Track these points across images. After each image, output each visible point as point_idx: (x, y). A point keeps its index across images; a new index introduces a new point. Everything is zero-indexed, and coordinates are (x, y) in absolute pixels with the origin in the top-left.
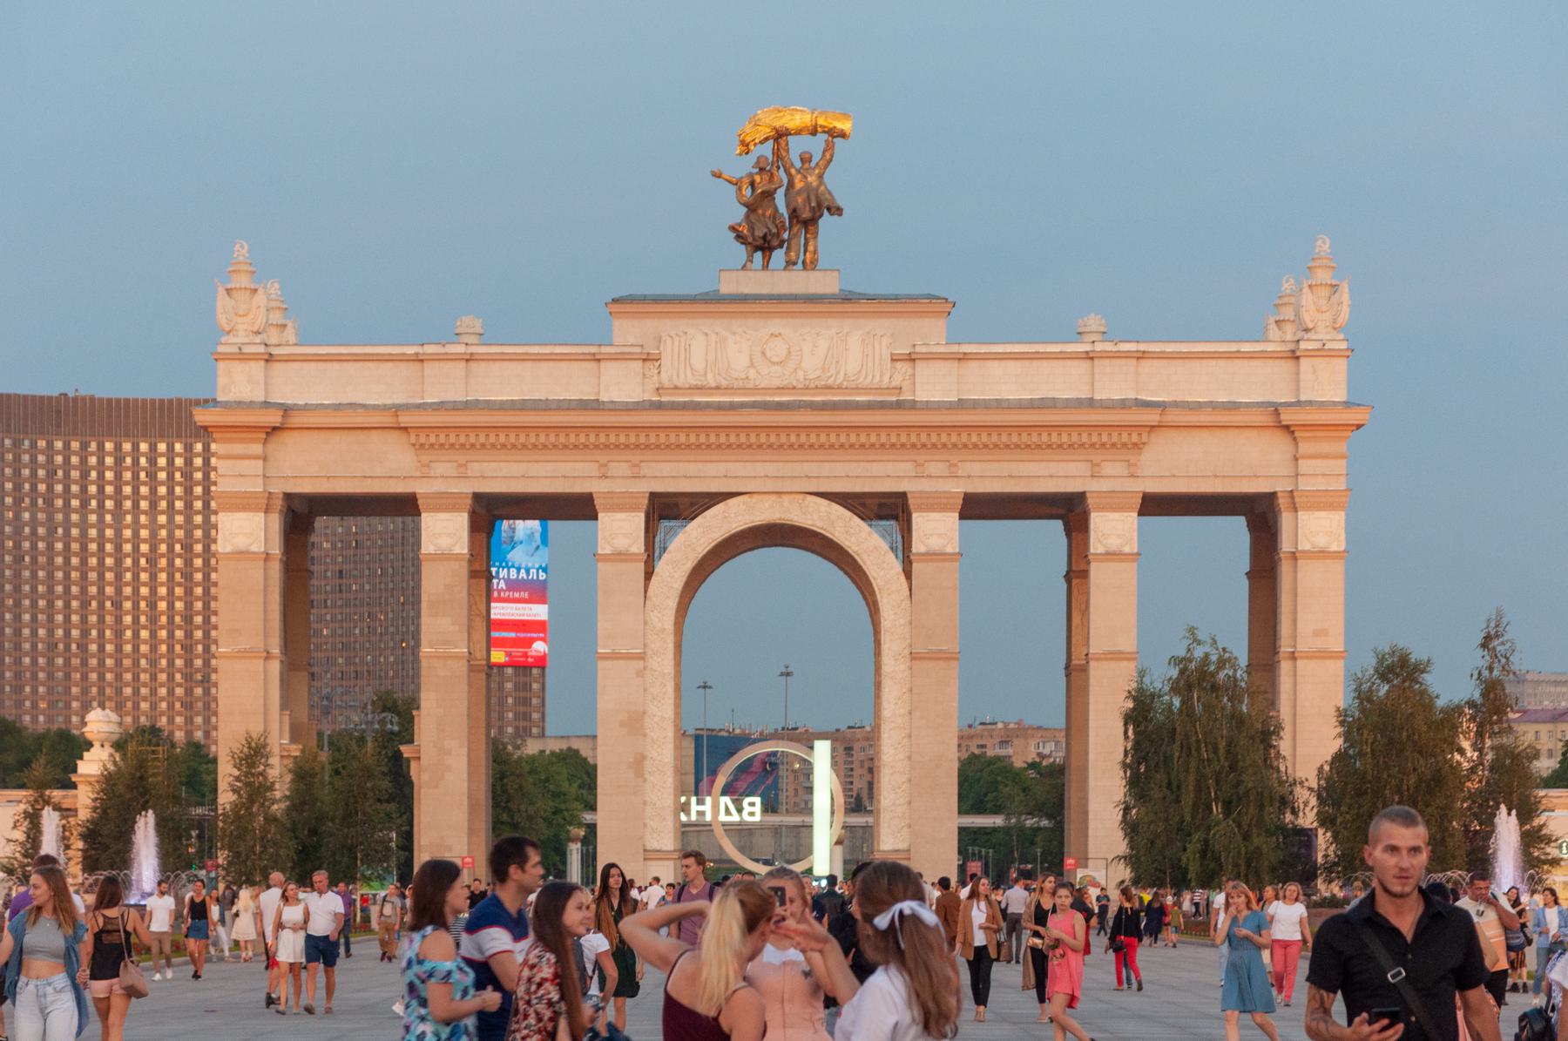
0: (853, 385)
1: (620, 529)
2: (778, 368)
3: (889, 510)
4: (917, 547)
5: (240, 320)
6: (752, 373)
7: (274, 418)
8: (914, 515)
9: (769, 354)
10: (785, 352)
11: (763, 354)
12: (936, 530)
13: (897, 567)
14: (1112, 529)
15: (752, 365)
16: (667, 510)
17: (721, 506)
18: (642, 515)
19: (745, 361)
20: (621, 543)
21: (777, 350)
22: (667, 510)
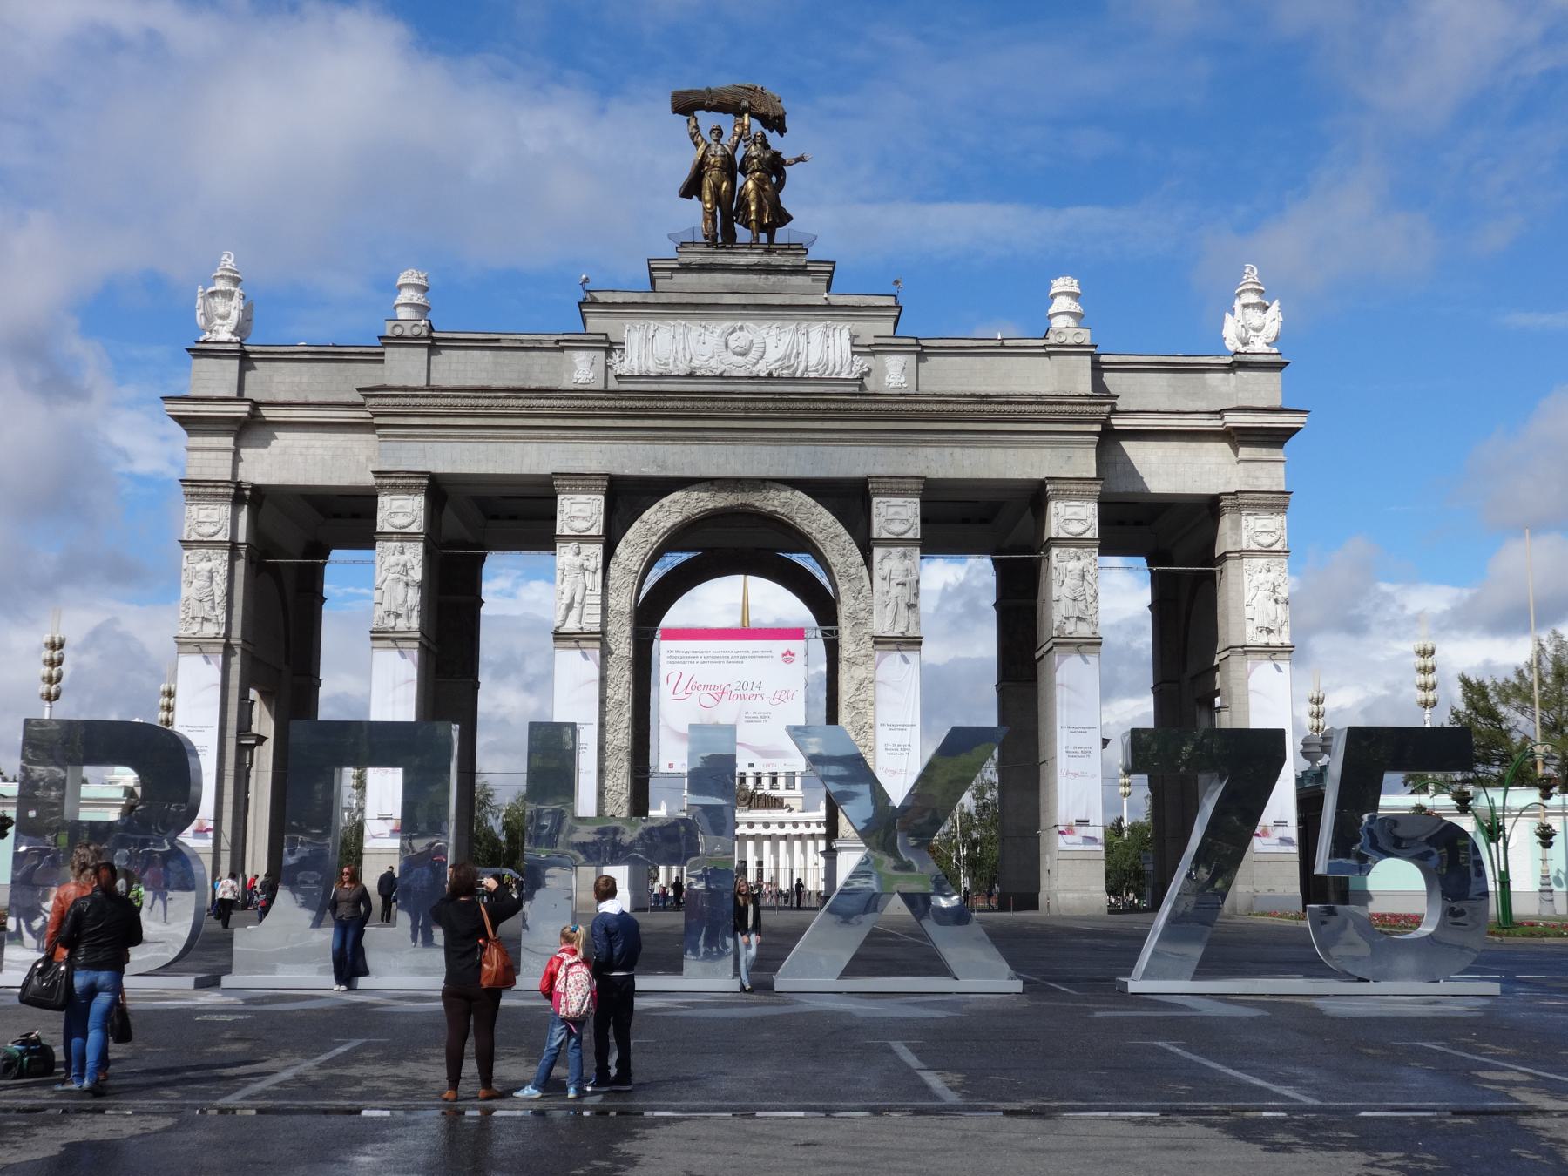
0: (812, 375)
1: (580, 512)
2: (740, 358)
3: (850, 500)
4: (878, 531)
5: (218, 321)
6: (713, 363)
7: (242, 410)
8: (875, 500)
9: (732, 344)
11: (727, 346)
12: (896, 515)
14: (1072, 517)
18: (602, 497)
20: (580, 525)
21: (739, 340)
22: (626, 498)
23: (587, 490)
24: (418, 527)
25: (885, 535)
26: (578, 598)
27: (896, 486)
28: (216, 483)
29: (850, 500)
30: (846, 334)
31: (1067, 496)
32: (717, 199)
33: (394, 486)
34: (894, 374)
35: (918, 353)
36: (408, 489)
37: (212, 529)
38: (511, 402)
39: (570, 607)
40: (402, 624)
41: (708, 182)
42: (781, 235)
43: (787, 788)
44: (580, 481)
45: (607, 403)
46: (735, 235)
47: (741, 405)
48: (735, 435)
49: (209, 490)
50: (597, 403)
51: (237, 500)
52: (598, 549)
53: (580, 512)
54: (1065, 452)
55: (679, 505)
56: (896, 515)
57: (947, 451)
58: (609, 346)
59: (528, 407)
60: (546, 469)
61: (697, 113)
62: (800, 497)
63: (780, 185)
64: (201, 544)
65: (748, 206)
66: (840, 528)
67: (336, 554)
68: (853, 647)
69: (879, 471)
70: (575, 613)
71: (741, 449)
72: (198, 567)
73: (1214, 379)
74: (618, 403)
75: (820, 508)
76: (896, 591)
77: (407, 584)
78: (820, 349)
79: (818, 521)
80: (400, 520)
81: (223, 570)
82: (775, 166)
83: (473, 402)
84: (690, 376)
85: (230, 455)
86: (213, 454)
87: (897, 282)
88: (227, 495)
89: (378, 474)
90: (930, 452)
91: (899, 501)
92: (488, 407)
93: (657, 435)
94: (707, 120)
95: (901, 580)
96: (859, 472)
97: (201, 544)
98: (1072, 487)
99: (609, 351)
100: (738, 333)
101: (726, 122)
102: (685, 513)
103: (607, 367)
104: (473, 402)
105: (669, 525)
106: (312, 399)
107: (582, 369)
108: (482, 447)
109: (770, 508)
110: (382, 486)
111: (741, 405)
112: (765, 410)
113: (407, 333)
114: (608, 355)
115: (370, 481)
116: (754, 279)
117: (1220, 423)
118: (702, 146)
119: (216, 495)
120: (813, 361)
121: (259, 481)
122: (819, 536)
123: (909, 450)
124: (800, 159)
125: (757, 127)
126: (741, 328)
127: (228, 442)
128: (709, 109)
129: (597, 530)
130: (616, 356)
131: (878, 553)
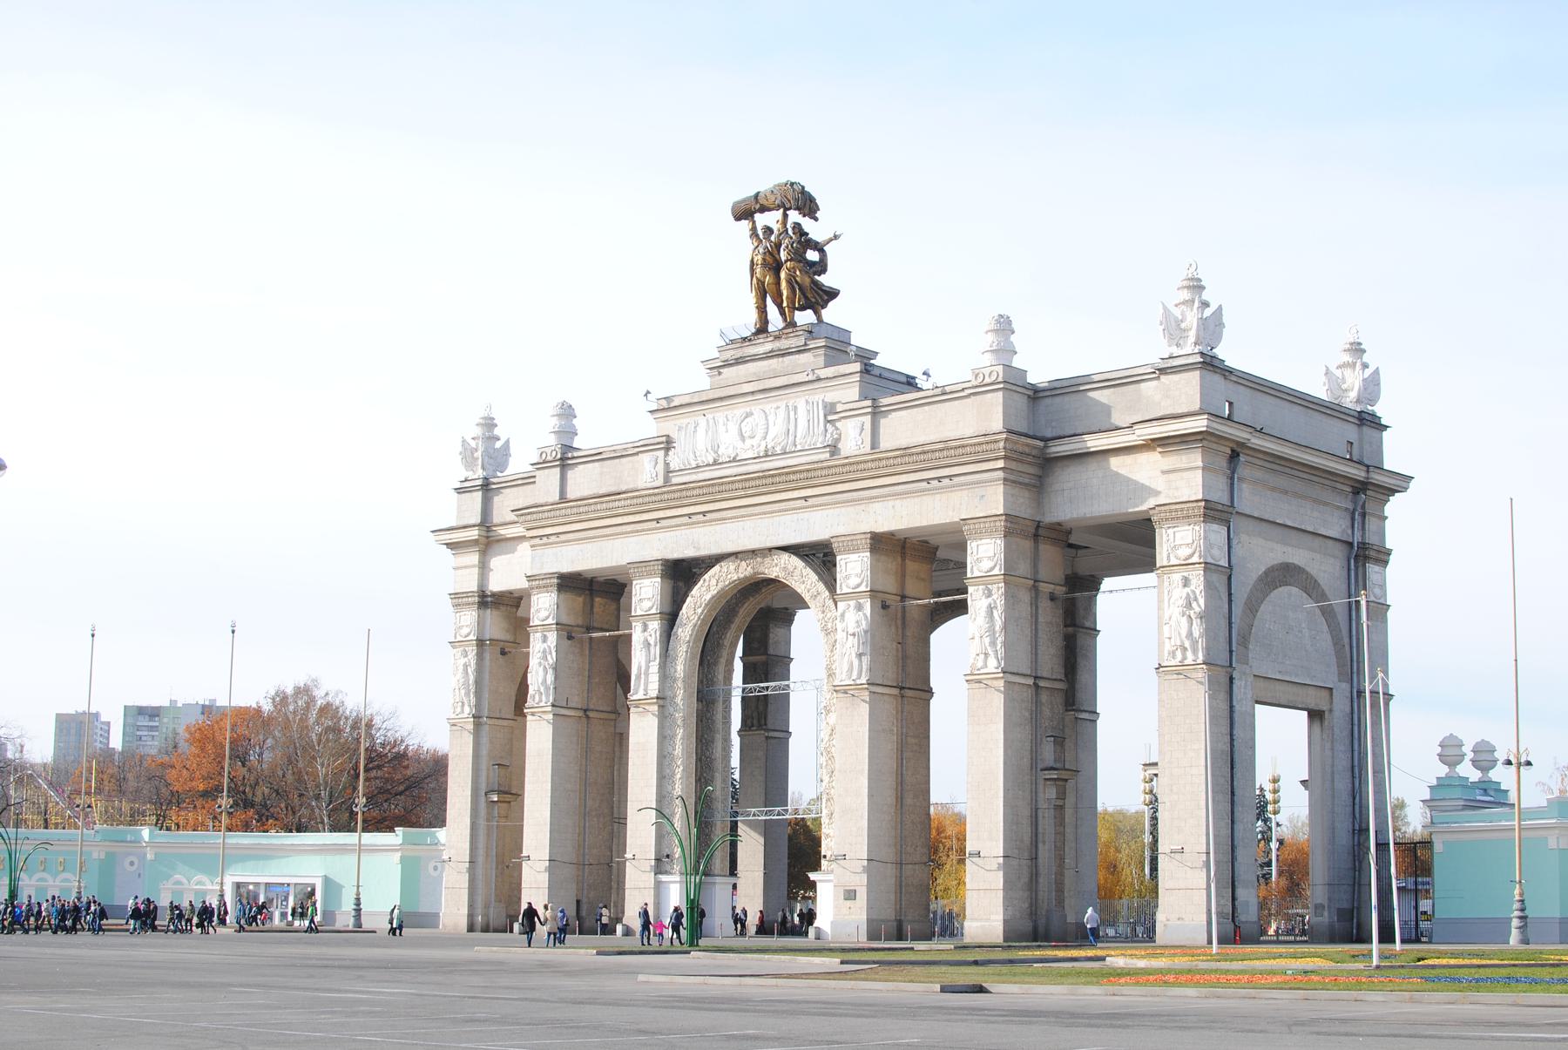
12: (854, 569)
17: (717, 568)
31: (980, 534)
34: (853, 437)
39: (639, 677)
44: (643, 566)
53: (647, 594)
54: (979, 491)
55: (714, 582)
56: (854, 569)
57: (891, 503)
61: (757, 216)
62: (795, 562)
63: (821, 267)
66: (821, 587)
67: (1108, 583)
69: (841, 530)
71: (748, 524)
73: (1148, 388)
75: (809, 570)
81: (473, 663)
85: (476, 570)
89: (530, 578)
94: (762, 220)
98: (980, 524)
99: (667, 449)
102: (721, 585)
103: (667, 464)
105: (708, 597)
114: (666, 455)
115: (524, 584)
116: (774, 363)
117: (1134, 437)
124: (836, 237)
125: (794, 216)
128: (763, 209)
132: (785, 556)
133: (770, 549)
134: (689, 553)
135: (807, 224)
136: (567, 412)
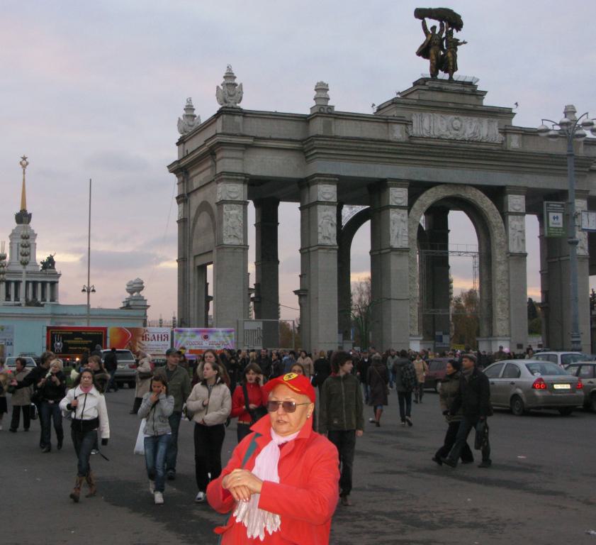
0: (485, 141)
1: (398, 195)
2: (457, 132)
3: (497, 194)
6: (448, 133)
7: (250, 141)
9: (455, 126)
10: (459, 126)
12: (516, 202)
13: (500, 219)
15: (448, 129)
16: (416, 189)
18: (407, 190)
19: (445, 127)
20: (399, 201)
21: (457, 123)
23: (401, 186)
24: (334, 199)
25: (513, 211)
26: (400, 233)
27: (516, 190)
28: (237, 174)
29: (497, 194)
30: (496, 124)
32: (437, 59)
33: (325, 181)
34: (514, 143)
35: (522, 134)
36: (330, 182)
37: (235, 196)
38: (373, 146)
39: (397, 237)
40: (327, 242)
41: (432, 51)
42: (457, 76)
43: (15, 301)
44: (398, 182)
45: (411, 149)
46: (437, 73)
47: (461, 153)
48: (458, 165)
49: (235, 177)
50: (407, 148)
51: (244, 182)
52: (406, 212)
53: (398, 195)
58: (408, 123)
59: (379, 149)
60: (384, 176)
61: (426, 19)
64: (232, 202)
65: (448, 63)
66: (495, 207)
68: (500, 257)
70: (399, 239)
72: (231, 212)
74: (415, 149)
75: (487, 198)
76: (518, 234)
77: (332, 224)
78: (486, 131)
79: (486, 204)
80: (327, 196)
82: (456, 43)
83: (358, 145)
84: (438, 138)
86: (234, 160)
87: (516, 104)
88: (241, 180)
90: (528, 176)
91: (517, 196)
92: (363, 147)
93: (427, 164)
94: (430, 23)
95: (520, 229)
96: (502, 183)
97: (232, 202)
100: (457, 121)
101: (437, 23)
104: (358, 145)
106: (273, 136)
107: (398, 133)
108: (358, 165)
109: (468, 197)
110: (320, 180)
111: (461, 153)
112: (470, 155)
113: (326, 111)
118: (430, 36)
119: (238, 180)
120: (485, 135)
121: (252, 173)
122: (486, 210)
123: (521, 175)
124: (465, 43)
126: (456, 119)
127: (239, 155)
128: (430, 17)
129: (405, 204)
130: (409, 127)
131: (510, 218)
132: (474, 191)
133: (465, 185)
134: (425, 179)
135: (456, 35)
136: (322, 89)
